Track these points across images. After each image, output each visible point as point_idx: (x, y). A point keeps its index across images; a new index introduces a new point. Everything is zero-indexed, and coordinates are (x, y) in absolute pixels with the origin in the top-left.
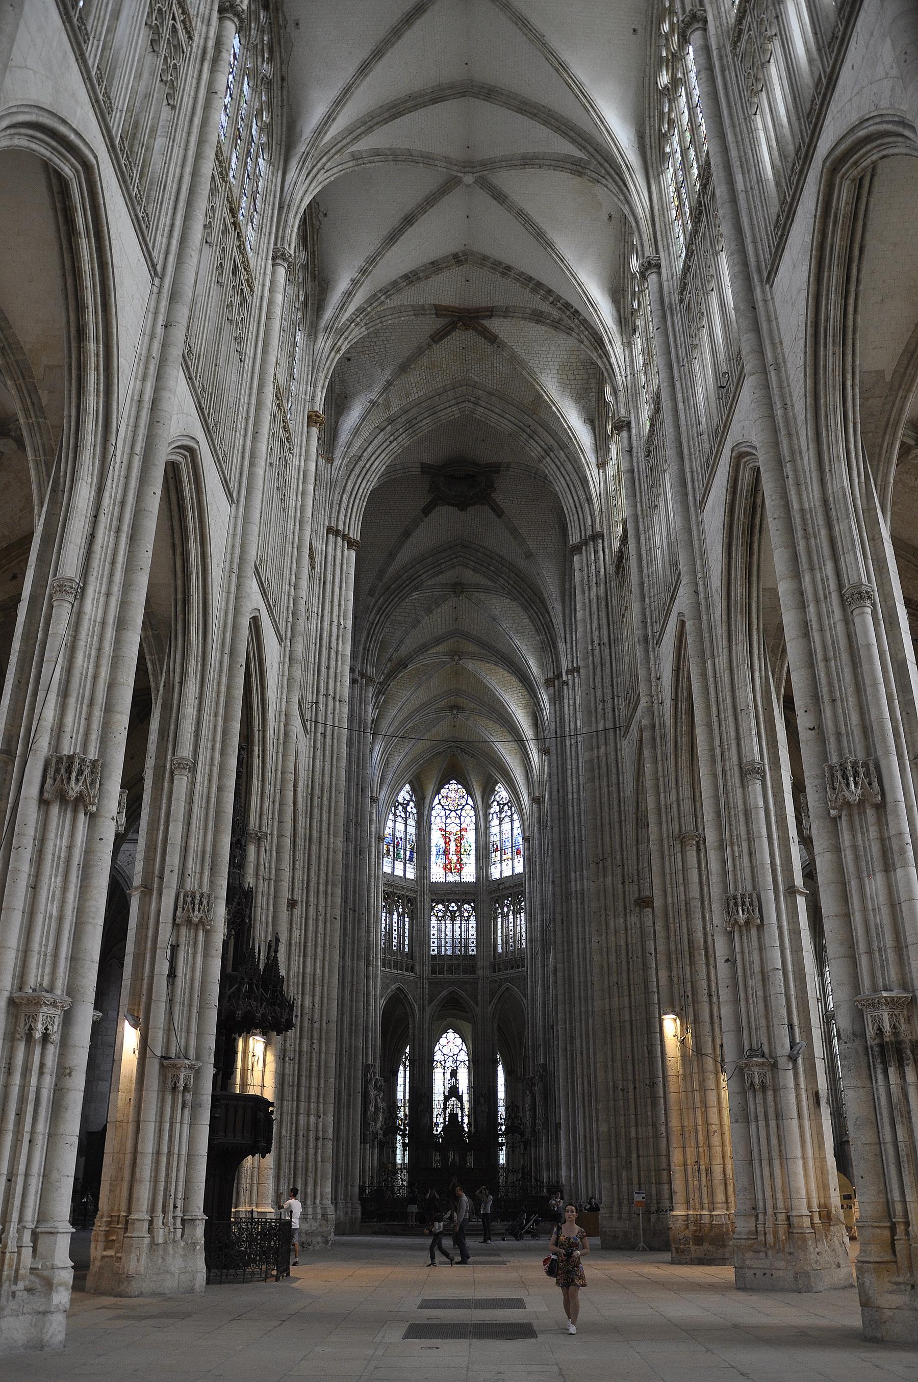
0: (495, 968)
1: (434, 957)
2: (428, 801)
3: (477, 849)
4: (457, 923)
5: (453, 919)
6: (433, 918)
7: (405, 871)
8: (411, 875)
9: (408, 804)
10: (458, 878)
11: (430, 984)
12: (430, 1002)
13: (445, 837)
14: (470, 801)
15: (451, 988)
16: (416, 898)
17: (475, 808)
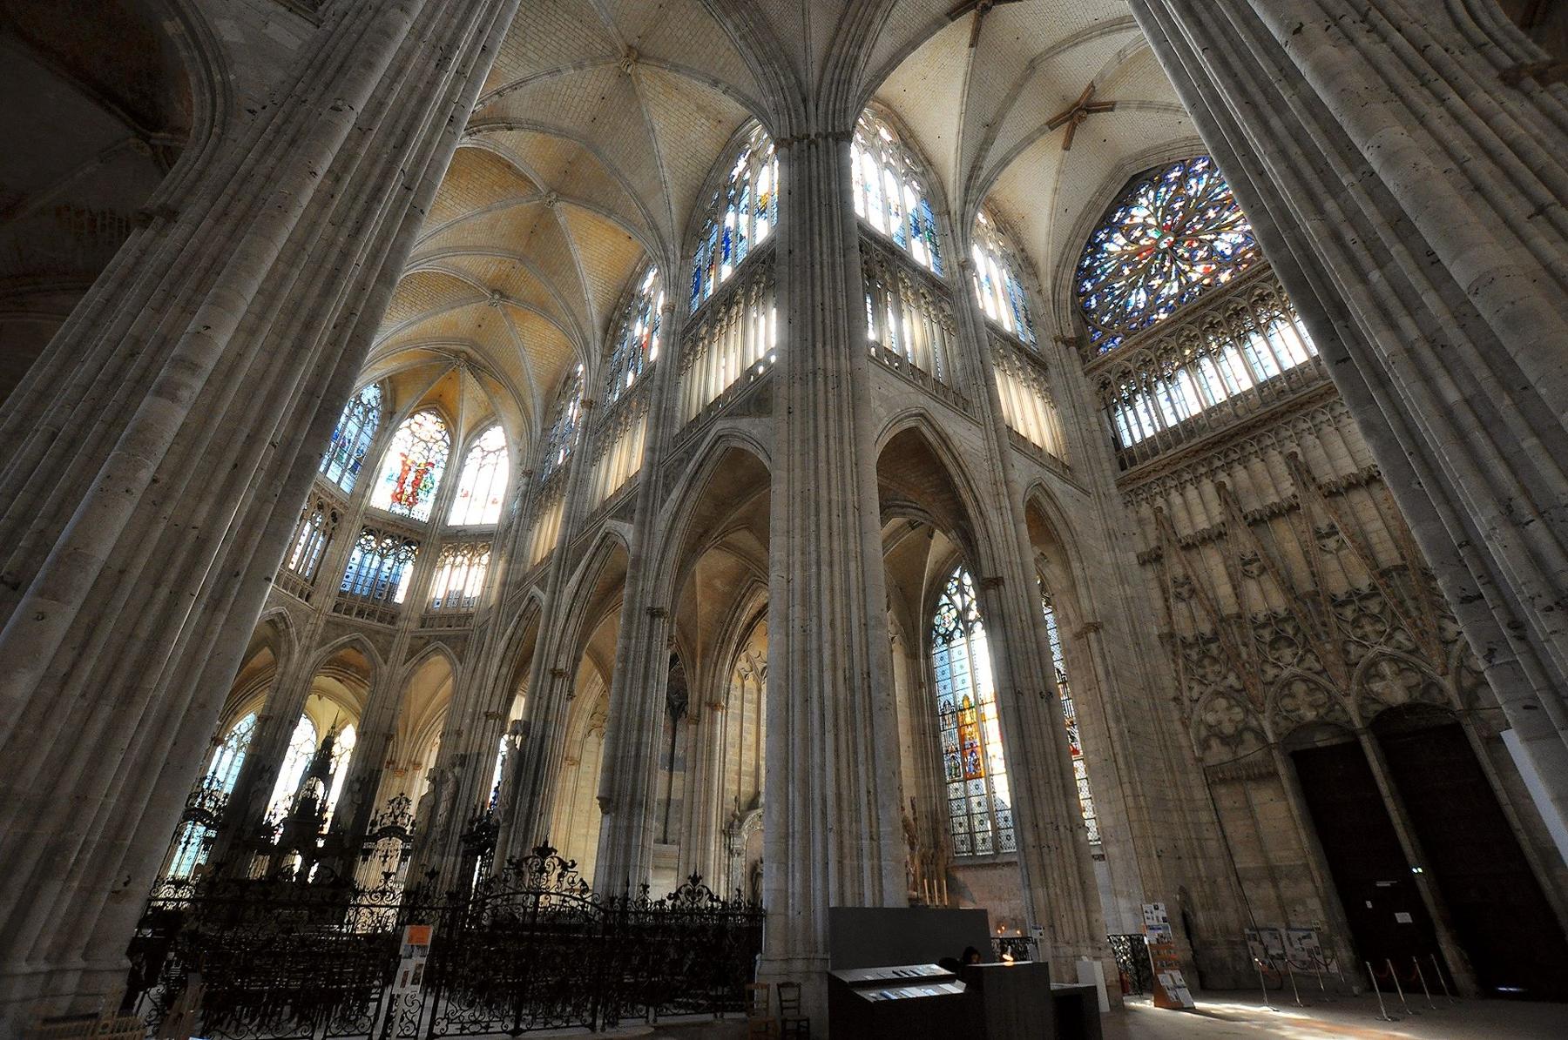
0: (423, 623)
1: (342, 594)
2: (396, 418)
3: (440, 488)
4: (389, 562)
5: (382, 556)
6: (357, 549)
7: (340, 479)
8: (346, 486)
9: (371, 410)
10: (406, 512)
11: (328, 622)
12: (323, 642)
13: (404, 463)
14: (447, 438)
15: (356, 635)
16: (340, 518)
17: (451, 447)
